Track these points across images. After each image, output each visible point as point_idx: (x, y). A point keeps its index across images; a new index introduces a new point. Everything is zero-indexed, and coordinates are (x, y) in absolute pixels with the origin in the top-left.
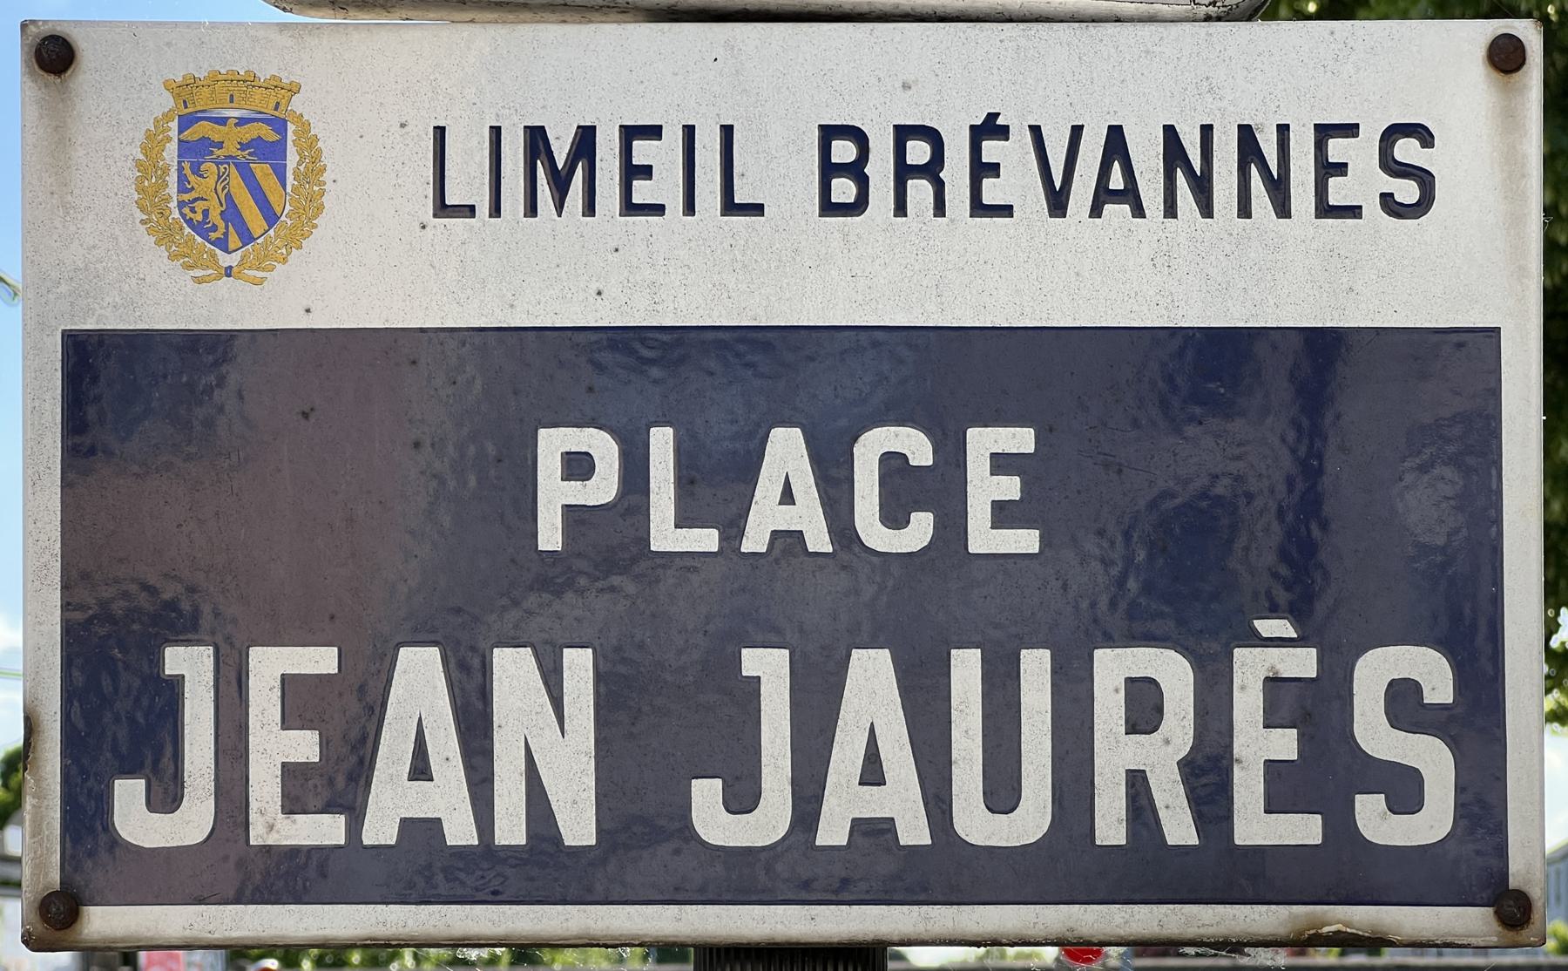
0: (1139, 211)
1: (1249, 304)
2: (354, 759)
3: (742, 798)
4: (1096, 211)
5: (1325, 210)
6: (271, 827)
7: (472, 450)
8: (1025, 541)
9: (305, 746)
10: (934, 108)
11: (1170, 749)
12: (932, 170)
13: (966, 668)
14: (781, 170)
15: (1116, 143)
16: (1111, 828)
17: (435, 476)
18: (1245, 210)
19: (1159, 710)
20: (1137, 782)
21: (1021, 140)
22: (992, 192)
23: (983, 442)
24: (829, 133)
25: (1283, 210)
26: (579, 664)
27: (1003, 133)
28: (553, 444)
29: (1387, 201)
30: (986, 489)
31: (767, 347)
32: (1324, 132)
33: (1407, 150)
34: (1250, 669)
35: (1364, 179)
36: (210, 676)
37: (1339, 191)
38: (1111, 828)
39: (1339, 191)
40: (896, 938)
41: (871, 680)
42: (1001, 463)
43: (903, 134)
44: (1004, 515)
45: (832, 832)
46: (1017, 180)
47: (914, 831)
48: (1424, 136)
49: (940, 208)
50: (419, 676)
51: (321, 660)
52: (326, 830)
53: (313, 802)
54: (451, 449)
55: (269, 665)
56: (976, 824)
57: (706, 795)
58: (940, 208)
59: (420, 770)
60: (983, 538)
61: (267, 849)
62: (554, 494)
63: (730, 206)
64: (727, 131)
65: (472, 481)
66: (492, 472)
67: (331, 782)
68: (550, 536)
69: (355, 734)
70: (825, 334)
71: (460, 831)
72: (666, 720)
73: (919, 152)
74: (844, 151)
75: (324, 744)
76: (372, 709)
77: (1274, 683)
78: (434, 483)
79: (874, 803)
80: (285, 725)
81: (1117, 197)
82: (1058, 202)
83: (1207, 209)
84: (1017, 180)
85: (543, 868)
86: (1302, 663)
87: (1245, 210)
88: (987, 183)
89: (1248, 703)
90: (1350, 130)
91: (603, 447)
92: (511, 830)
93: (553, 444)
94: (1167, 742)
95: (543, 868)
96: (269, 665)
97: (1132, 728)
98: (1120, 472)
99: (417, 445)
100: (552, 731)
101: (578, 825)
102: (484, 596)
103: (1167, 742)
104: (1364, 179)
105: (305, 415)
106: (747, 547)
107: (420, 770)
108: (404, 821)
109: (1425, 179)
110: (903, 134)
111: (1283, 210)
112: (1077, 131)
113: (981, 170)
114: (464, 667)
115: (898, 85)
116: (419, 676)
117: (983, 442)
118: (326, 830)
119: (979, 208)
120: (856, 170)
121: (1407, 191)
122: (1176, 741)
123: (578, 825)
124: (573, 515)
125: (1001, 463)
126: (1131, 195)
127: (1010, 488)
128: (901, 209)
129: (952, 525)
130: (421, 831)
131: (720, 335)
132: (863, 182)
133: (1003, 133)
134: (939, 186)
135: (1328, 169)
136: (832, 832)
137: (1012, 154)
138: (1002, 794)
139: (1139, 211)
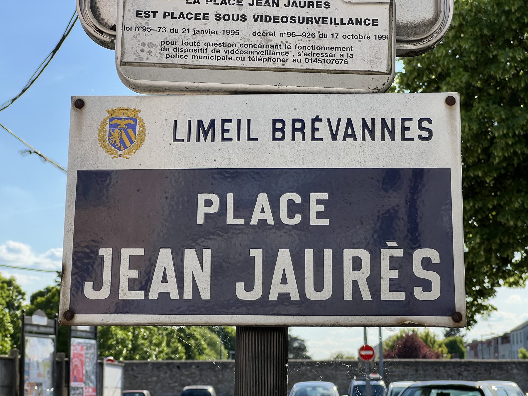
0: (355, 139)
1: (384, 162)
2: (147, 277)
3: (249, 287)
4: (344, 139)
5: (404, 139)
6: (125, 294)
7: (181, 199)
8: (325, 222)
9: (135, 274)
10: (302, 114)
11: (364, 275)
12: (302, 130)
13: (309, 254)
14: (263, 130)
15: (349, 123)
16: (348, 295)
17: (171, 206)
18: (383, 139)
19: (361, 265)
20: (355, 284)
21: (325, 123)
22: (317, 135)
23: (314, 197)
24: (275, 121)
25: (393, 139)
26: (207, 253)
27: (320, 120)
28: (202, 197)
29: (420, 137)
30: (315, 209)
31: (258, 173)
32: (403, 120)
33: (425, 124)
34: (385, 254)
35: (414, 131)
36: (111, 256)
37: (407, 134)
38: (348, 295)
39: (407, 134)
40: (290, 324)
41: (284, 257)
42: (319, 202)
43: (294, 121)
44: (320, 215)
45: (273, 296)
46: (324, 131)
47: (295, 296)
48: (429, 121)
49: (304, 139)
50: (165, 257)
51: (140, 252)
52: (139, 295)
53: (136, 288)
54: (175, 199)
55: (126, 253)
56: (311, 294)
57: (240, 287)
58: (304, 139)
59: (165, 279)
60: (314, 221)
61: (124, 300)
62: (202, 210)
63: (249, 139)
64: (249, 121)
65: (181, 207)
66: (186, 205)
67: (141, 283)
68: (200, 220)
69: (147, 270)
70: (274, 170)
71: (174, 295)
72: (229, 269)
73: (298, 125)
74: (279, 125)
75: (140, 273)
76: (152, 264)
77: (391, 258)
78: (171, 208)
79: (284, 289)
80: (130, 268)
81: (350, 136)
82: (334, 137)
83: (373, 139)
84: (324, 131)
85: (196, 306)
86: (399, 253)
87: (383, 139)
88: (316, 133)
89: (385, 263)
90: (410, 119)
91: (215, 198)
92: (188, 295)
93: (202, 197)
94: (363, 273)
95: (196, 306)
96: (126, 253)
97: (354, 269)
98: (350, 204)
99: (167, 198)
100: (199, 268)
101: (206, 294)
102: (184, 235)
103: (363, 273)
104: (414, 131)
105: (138, 191)
106: (252, 223)
107: (165, 279)
108: (160, 293)
109: (430, 131)
110: (294, 121)
111: (393, 139)
112: (339, 120)
113: (314, 129)
114: (177, 254)
115: (293, 109)
116: (165, 257)
117: (314, 197)
118: (139, 295)
119: (314, 139)
120: (282, 130)
121: (425, 134)
122: (365, 273)
123: (206, 294)
124: (207, 215)
125: (319, 202)
126: (353, 136)
127: (321, 208)
128: (293, 139)
129: (306, 218)
130: (164, 296)
131: (246, 170)
132: (284, 133)
133: (320, 120)
134: (303, 134)
135: (404, 129)
136: (273, 296)
137: (322, 126)
138: (319, 286)
139: (355, 139)
